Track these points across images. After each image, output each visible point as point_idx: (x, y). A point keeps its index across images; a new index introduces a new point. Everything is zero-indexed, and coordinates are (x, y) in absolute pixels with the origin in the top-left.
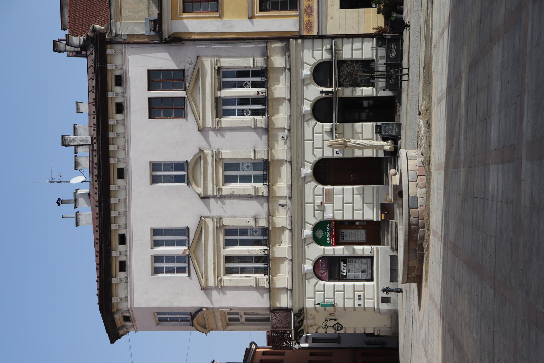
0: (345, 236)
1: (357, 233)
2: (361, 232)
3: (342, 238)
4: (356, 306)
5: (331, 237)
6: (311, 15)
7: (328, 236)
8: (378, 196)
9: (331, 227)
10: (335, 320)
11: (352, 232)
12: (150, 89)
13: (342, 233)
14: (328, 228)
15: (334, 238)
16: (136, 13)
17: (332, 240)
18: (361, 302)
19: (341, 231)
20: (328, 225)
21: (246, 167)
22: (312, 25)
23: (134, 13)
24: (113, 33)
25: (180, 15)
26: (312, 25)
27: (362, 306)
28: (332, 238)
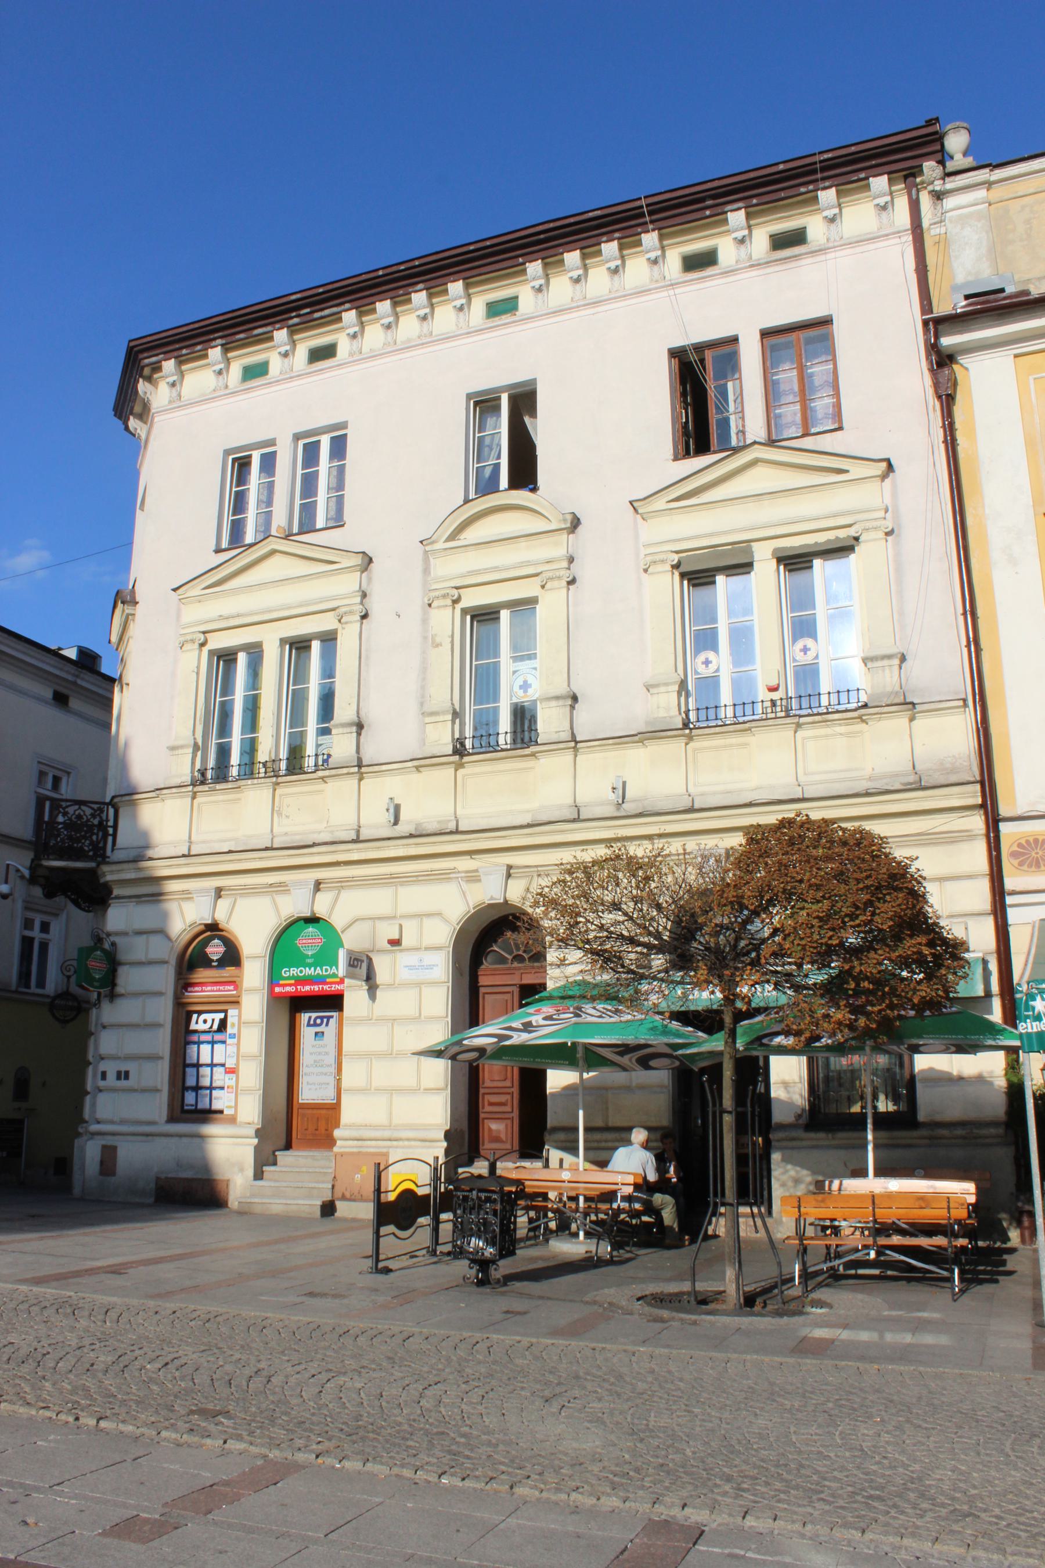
0: (318, 1029)
1: (325, 1070)
3: (312, 1022)
4: (103, 1066)
7: (301, 971)
8: (413, 1143)
9: (328, 980)
11: (327, 1053)
12: (765, 334)
14: (326, 970)
15: (297, 989)
17: (290, 985)
19: (332, 1017)
21: (525, 682)
24: (944, 183)
25: (1035, 379)
27: (102, 1084)
28: (295, 985)
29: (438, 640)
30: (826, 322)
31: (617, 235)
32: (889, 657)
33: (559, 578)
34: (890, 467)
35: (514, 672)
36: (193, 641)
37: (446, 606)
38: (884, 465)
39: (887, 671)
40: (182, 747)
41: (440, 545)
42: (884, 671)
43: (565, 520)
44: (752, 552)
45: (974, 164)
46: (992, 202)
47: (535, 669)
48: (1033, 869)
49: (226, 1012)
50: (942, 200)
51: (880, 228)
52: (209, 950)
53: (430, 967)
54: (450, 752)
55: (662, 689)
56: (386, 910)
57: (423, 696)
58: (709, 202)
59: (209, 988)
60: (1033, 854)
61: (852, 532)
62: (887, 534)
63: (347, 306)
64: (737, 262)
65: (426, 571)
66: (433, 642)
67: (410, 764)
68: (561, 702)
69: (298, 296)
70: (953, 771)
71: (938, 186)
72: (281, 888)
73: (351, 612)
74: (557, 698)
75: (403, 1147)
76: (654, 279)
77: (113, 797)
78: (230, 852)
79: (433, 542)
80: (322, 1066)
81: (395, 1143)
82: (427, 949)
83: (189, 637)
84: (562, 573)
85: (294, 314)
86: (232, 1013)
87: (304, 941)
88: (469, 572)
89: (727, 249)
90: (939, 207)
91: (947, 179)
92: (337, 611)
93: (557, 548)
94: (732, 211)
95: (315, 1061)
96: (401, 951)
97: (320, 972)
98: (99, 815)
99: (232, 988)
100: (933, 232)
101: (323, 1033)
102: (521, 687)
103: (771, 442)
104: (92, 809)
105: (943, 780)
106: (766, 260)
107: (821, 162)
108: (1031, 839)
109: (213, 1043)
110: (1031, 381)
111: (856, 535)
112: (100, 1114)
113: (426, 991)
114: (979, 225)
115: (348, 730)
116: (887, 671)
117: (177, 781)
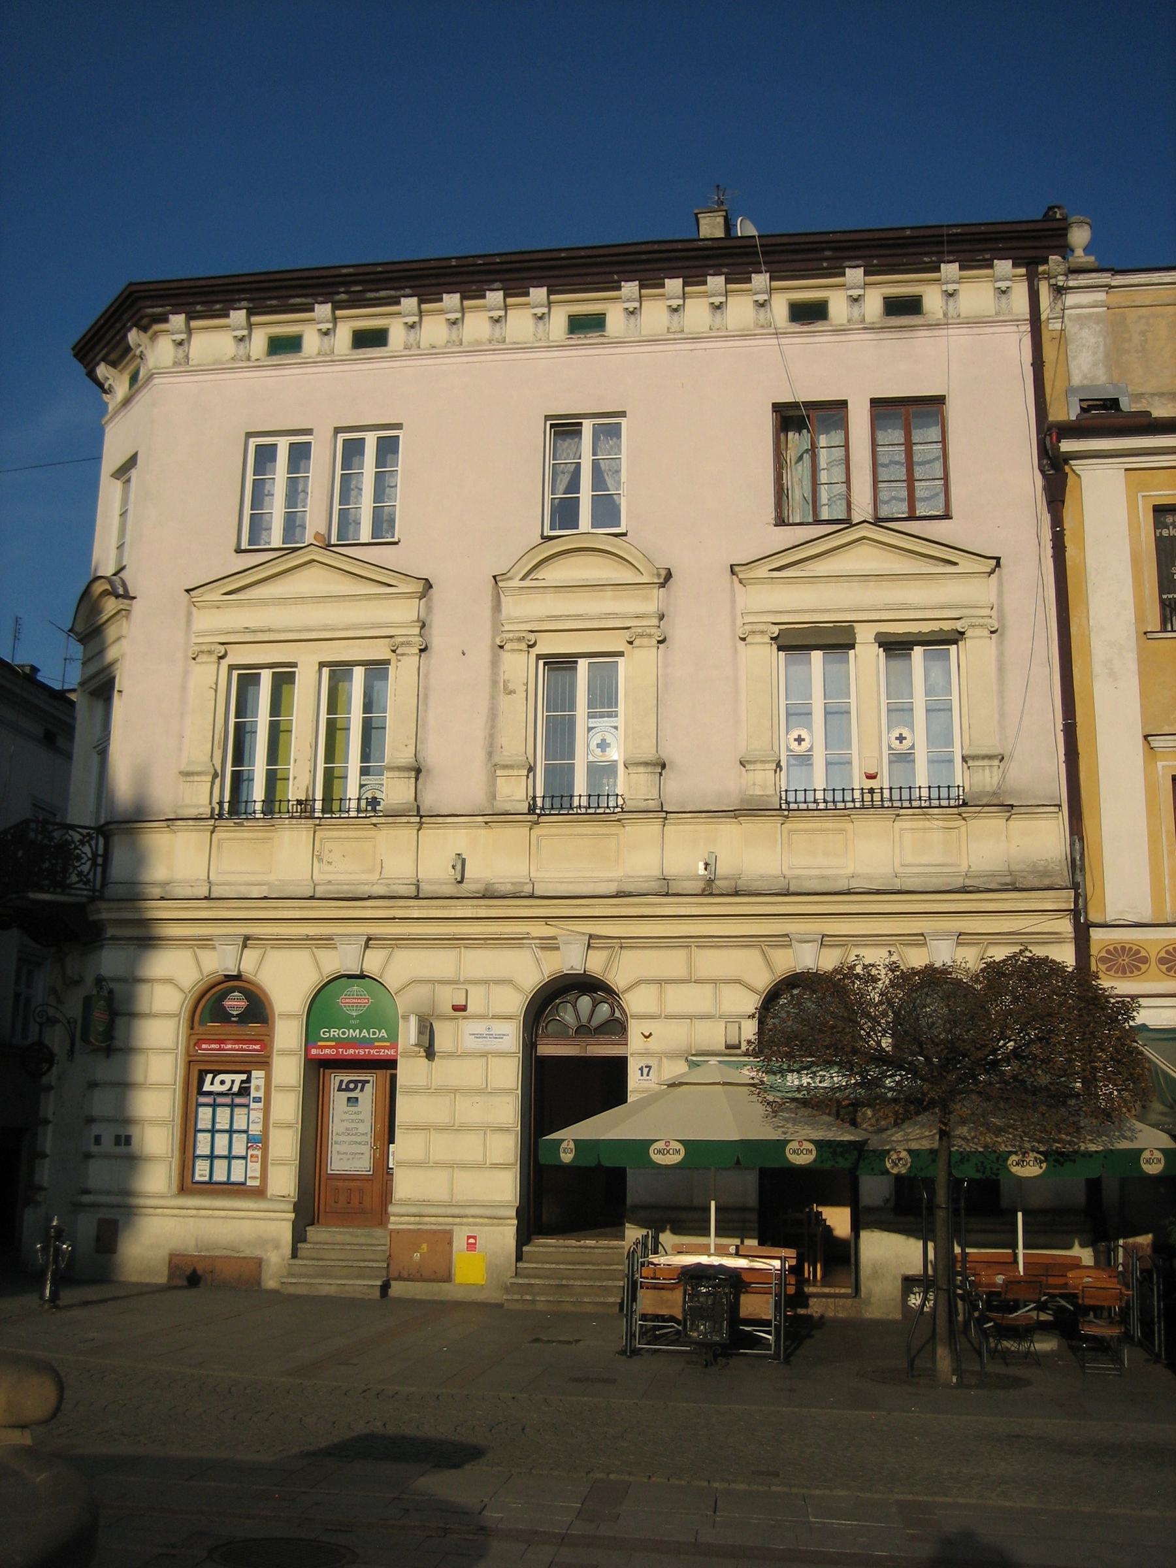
1: (358, 1139)
2: (362, 1154)
3: (344, 1087)
4: (96, 1129)
5: (341, 1043)
6: (1169, 970)
8: (478, 1220)
9: (376, 1044)
10: (71, 1052)
11: (362, 1121)
12: (875, 402)
13: (360, 1085)
14: (374, 1033)
15: (338, 1052)
16: (1140, 354)
18: (108, 1145)
19: (368, 1082)
20: (384, 1033)
21: (603, 740)
22: (1128, 974)
23: (1140, 348)
24: (1067, 280)
25: (1143, 496)
26: (1132, 972)
27: (94, 1149)
29: (511, 687)
30: (940, 400)
31: (725, 270)
32: (990, 757)
33: (650, 636)
34: (998, 565)
35: (590, 729)
36: (210, 652)
37: (521, 650)
38: (994, 562)
39: (987, 771)
40: (199, 774)
41: (516, 583)
42: (984, 770)
43: (659, 575)
44: (855, 634)
45: (1096, 265)
46: (1111, 306)
47: (616, 728)
48: (1120, 974)
49: (249, 1073)
50: (1062, 295)
51: (997, 314)
52: (227, 1003)
53: (501, 1036)
54: (526, 811)
55: (759, 766)
56: (448, 973)
57: (491, 745)
58: (828, 253)
59: (229, 1046)
60: (1120, 960)
61: (958, 625)
62: (992, 632)
63: (408, 291)
64: (849, 321)
65: (497, 607)
66: (505, 687)
67: (480, 819)
68: (650, 769)
69: (351, 270)
70: (1046, 873)
71: (1061, 281)
72: (326, 942)
73: (408, 644)
74: (646, 764)
75: (469, 1224)
76: (760, 324)
77: (107, 823)
78: (265, 898)
79: (509, 579)
80: (356, 1134)
81: (458, 1220)
82: (494, 1017)
83: (205, 648)
84: (653, 631)
85: (342, 289)
86: (258, 1076)
87: (347, 1001)
88: (548, 617)
89: (838, 306)
90: (1060, 302)
91: (1071, 277)
92: (393, 640)
93: (647, 604)
94: (850, 267)
95: (347, 1129)
96: (465, 1018)
97: (367, 1035)
98: (88, 841)
99: (257, 1047)
100: (1051, 327)
101: (357, 1099)
102: (598, 746)
103: (878, 521)
104: (81, 834)
105: (1036, 884)
106: (880, 326)
107: (948, 235)
108: (1119, 946)
109: (232, 1106)
110: (1140, 499)
111: (963, 630)
112: (92, 1184)
113: (494, 1062)
114: (1098, 329)
115: (406, 774)
116: (987, 771)
117: (193, 812)
